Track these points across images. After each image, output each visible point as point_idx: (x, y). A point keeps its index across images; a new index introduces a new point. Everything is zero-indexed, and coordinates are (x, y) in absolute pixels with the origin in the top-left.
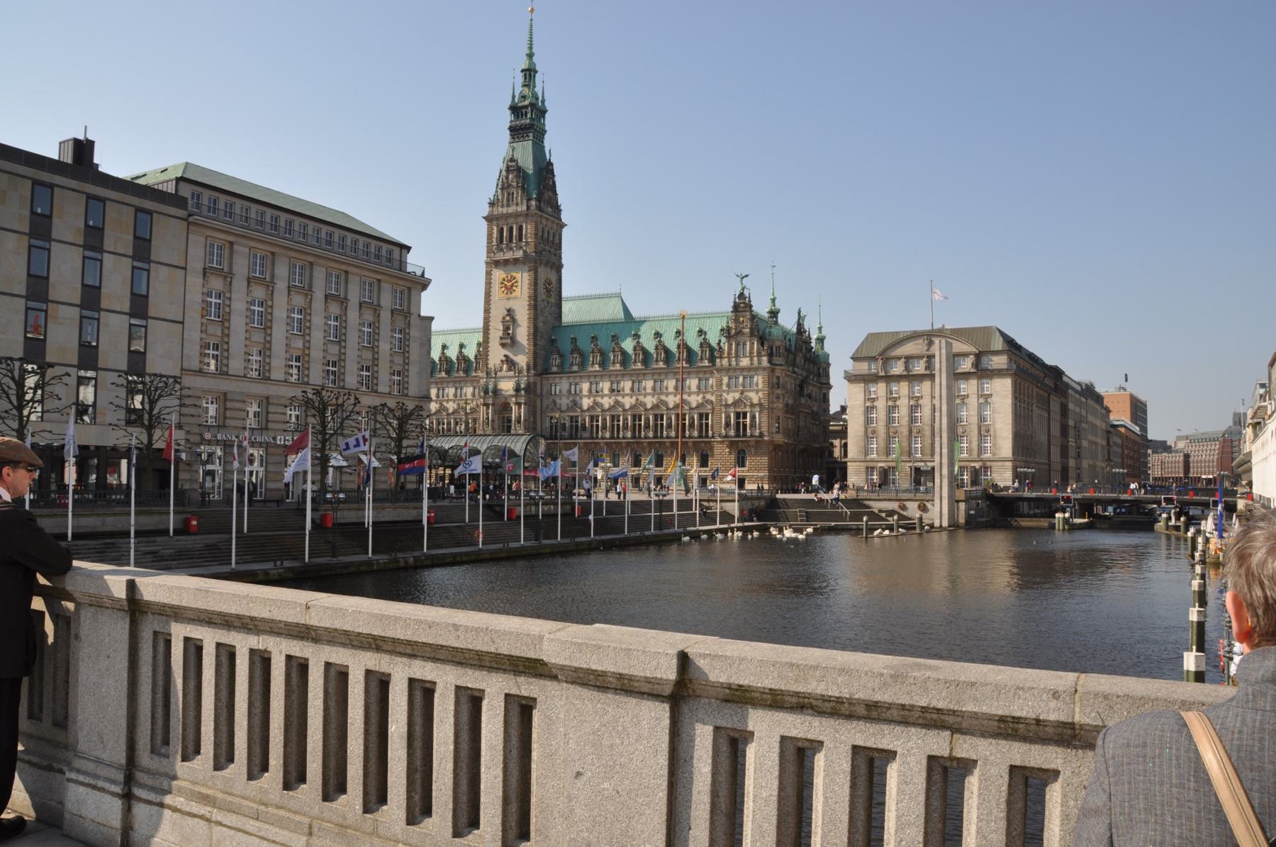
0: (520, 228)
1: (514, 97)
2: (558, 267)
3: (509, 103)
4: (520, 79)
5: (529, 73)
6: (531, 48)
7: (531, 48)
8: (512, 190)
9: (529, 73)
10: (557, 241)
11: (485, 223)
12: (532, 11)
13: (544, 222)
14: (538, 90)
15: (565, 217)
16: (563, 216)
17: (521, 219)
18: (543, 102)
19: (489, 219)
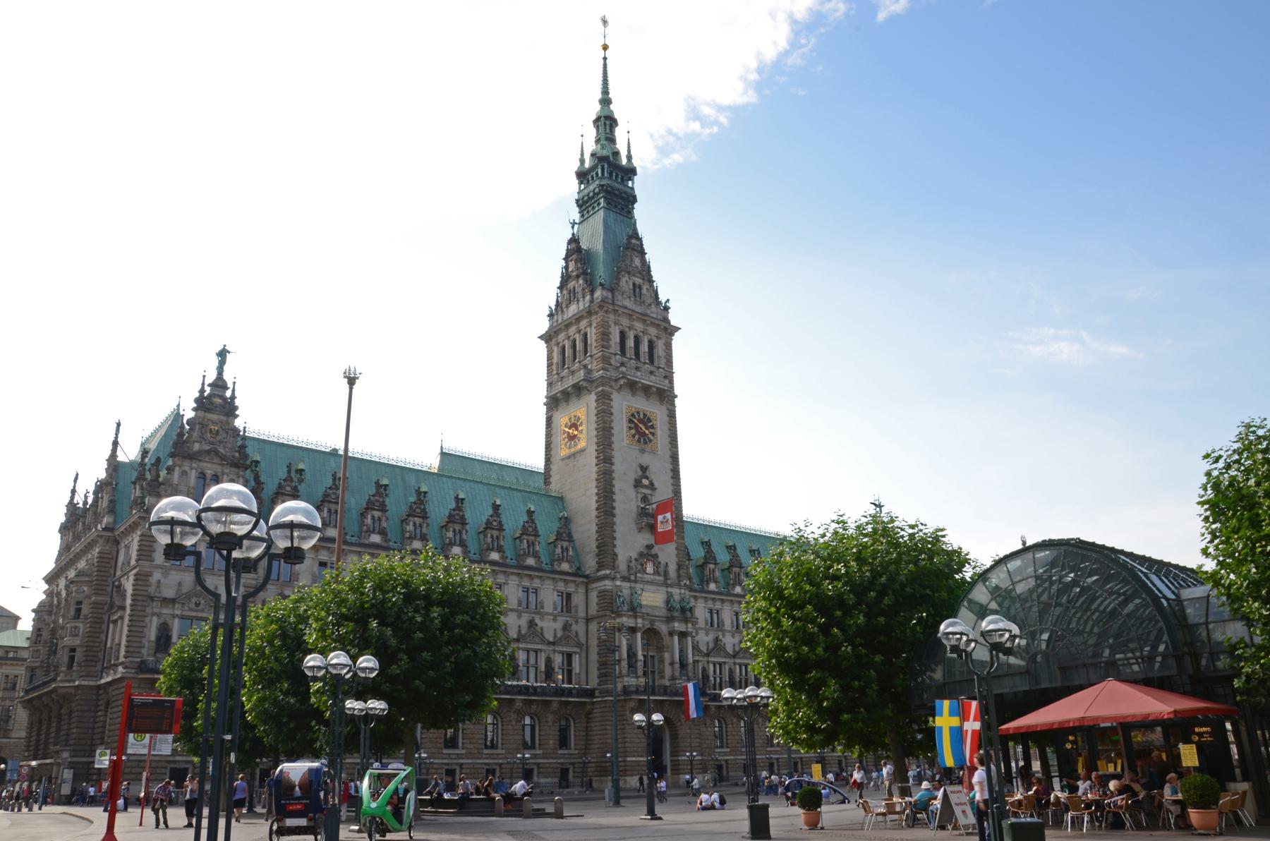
0: (586, 334)
1: (582, 161)
2: (666, 396)
3: (576, 165)
4: (591, 133)
5: (606, 123)
6: (605, 91)
7: (605, 91)
8: (571, 285)
9: (606, 123)
10: (660, 349)
11: (542, 347)
12: (605, 48)
13: (625, 322)
14: (621, 146)
15: (674, 319)
16: (671, 317)
17: (584, 323)
18: (629, 157)
19: (548, 338)
